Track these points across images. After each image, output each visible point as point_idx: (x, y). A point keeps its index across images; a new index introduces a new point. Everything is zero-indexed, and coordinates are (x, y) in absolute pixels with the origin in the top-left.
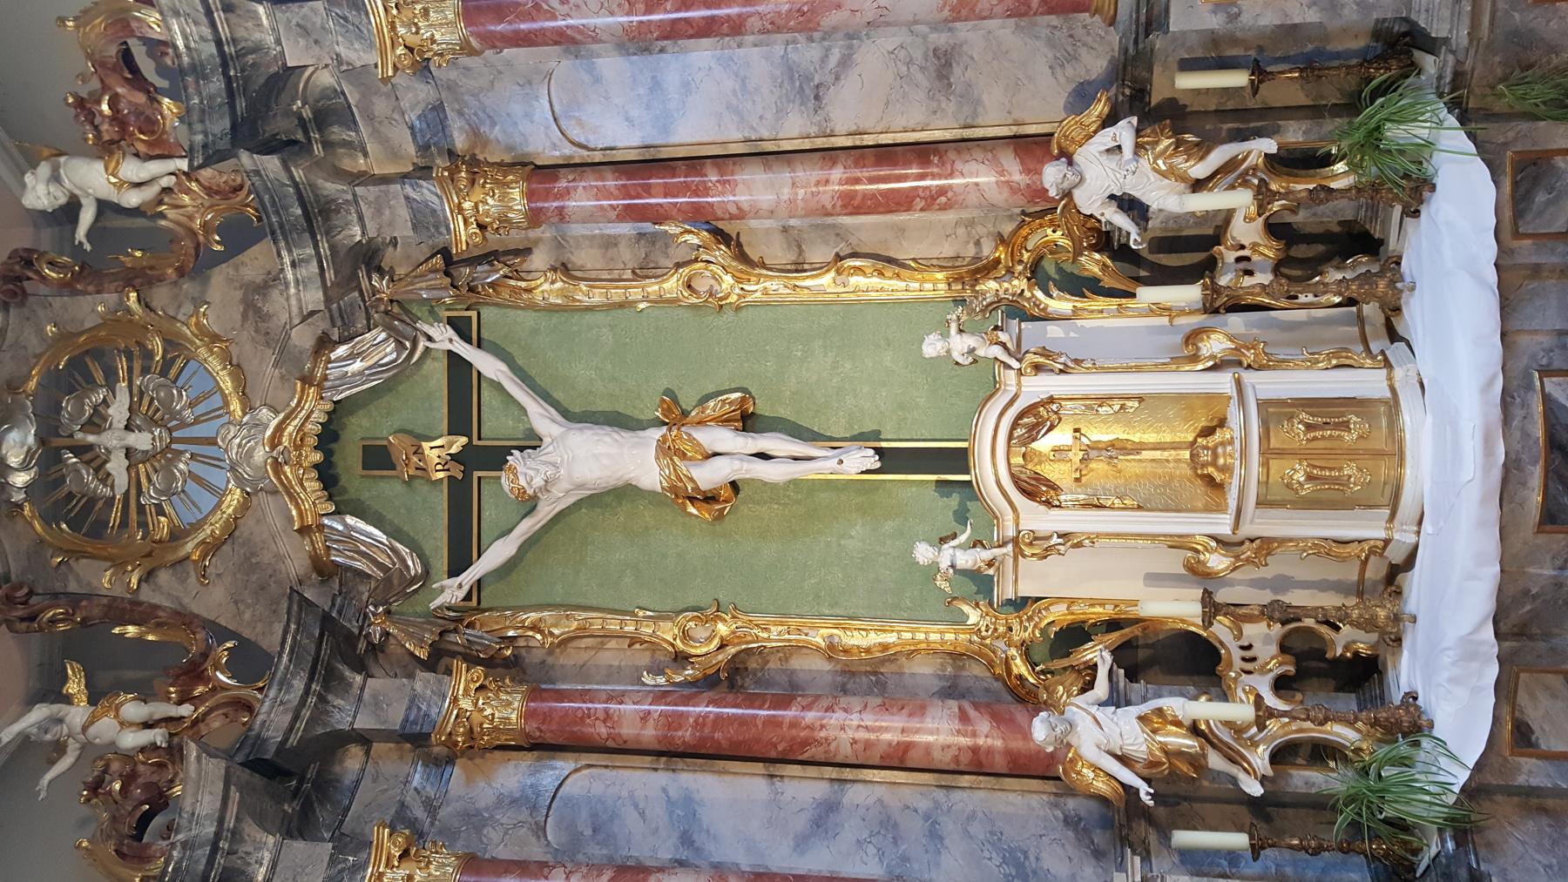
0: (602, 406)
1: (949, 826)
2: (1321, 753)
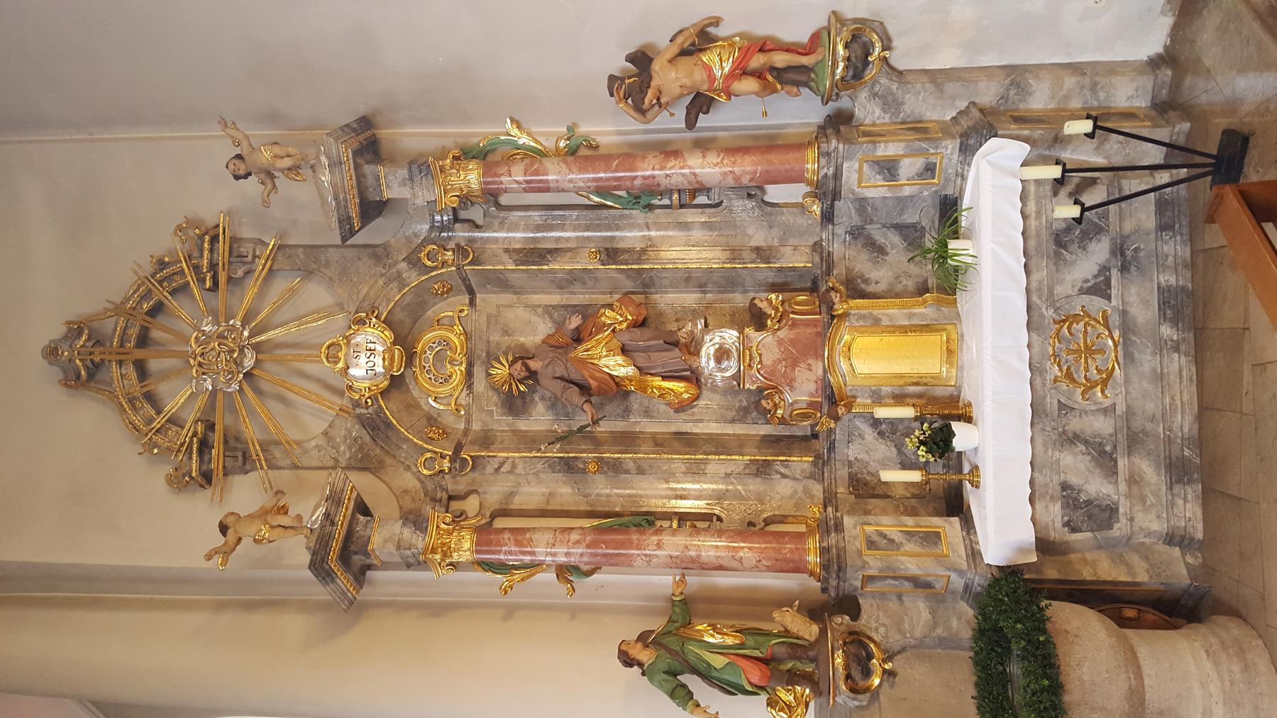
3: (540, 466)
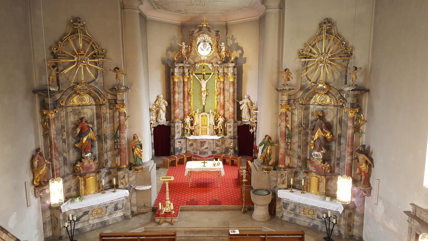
0: (208, 85)
1: (181, 110)
2: (187, 132)
3: (300, 120)
